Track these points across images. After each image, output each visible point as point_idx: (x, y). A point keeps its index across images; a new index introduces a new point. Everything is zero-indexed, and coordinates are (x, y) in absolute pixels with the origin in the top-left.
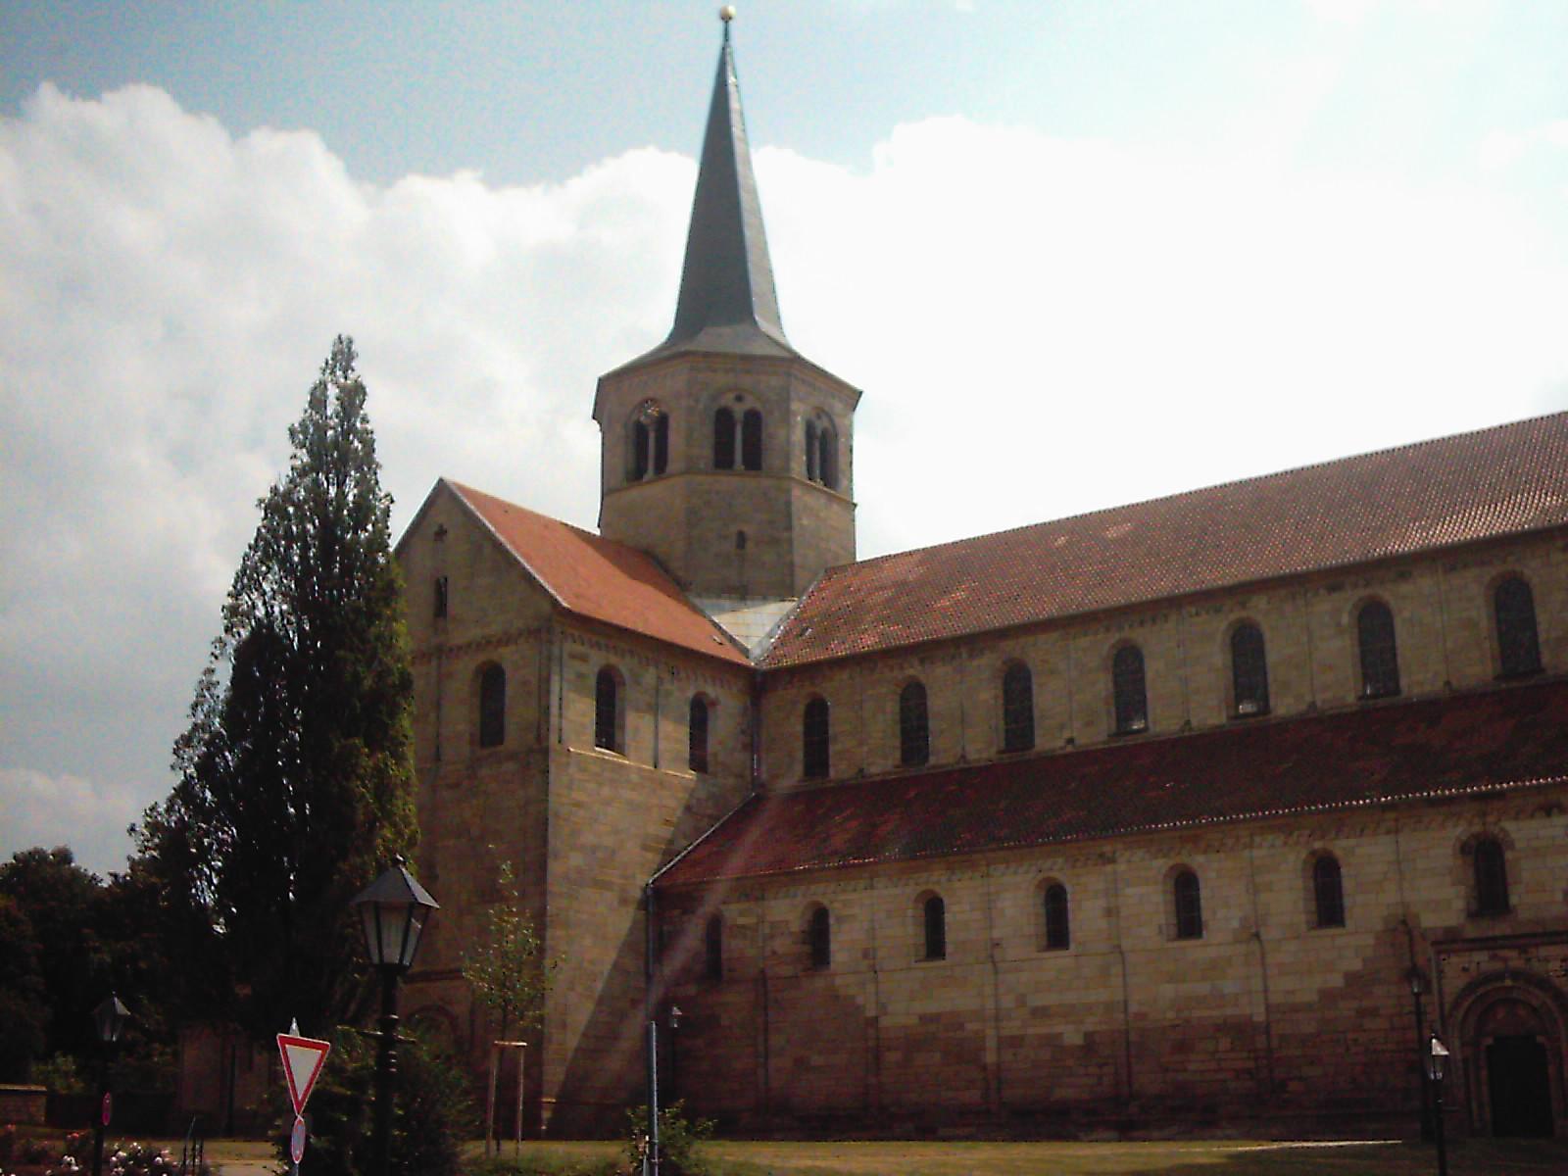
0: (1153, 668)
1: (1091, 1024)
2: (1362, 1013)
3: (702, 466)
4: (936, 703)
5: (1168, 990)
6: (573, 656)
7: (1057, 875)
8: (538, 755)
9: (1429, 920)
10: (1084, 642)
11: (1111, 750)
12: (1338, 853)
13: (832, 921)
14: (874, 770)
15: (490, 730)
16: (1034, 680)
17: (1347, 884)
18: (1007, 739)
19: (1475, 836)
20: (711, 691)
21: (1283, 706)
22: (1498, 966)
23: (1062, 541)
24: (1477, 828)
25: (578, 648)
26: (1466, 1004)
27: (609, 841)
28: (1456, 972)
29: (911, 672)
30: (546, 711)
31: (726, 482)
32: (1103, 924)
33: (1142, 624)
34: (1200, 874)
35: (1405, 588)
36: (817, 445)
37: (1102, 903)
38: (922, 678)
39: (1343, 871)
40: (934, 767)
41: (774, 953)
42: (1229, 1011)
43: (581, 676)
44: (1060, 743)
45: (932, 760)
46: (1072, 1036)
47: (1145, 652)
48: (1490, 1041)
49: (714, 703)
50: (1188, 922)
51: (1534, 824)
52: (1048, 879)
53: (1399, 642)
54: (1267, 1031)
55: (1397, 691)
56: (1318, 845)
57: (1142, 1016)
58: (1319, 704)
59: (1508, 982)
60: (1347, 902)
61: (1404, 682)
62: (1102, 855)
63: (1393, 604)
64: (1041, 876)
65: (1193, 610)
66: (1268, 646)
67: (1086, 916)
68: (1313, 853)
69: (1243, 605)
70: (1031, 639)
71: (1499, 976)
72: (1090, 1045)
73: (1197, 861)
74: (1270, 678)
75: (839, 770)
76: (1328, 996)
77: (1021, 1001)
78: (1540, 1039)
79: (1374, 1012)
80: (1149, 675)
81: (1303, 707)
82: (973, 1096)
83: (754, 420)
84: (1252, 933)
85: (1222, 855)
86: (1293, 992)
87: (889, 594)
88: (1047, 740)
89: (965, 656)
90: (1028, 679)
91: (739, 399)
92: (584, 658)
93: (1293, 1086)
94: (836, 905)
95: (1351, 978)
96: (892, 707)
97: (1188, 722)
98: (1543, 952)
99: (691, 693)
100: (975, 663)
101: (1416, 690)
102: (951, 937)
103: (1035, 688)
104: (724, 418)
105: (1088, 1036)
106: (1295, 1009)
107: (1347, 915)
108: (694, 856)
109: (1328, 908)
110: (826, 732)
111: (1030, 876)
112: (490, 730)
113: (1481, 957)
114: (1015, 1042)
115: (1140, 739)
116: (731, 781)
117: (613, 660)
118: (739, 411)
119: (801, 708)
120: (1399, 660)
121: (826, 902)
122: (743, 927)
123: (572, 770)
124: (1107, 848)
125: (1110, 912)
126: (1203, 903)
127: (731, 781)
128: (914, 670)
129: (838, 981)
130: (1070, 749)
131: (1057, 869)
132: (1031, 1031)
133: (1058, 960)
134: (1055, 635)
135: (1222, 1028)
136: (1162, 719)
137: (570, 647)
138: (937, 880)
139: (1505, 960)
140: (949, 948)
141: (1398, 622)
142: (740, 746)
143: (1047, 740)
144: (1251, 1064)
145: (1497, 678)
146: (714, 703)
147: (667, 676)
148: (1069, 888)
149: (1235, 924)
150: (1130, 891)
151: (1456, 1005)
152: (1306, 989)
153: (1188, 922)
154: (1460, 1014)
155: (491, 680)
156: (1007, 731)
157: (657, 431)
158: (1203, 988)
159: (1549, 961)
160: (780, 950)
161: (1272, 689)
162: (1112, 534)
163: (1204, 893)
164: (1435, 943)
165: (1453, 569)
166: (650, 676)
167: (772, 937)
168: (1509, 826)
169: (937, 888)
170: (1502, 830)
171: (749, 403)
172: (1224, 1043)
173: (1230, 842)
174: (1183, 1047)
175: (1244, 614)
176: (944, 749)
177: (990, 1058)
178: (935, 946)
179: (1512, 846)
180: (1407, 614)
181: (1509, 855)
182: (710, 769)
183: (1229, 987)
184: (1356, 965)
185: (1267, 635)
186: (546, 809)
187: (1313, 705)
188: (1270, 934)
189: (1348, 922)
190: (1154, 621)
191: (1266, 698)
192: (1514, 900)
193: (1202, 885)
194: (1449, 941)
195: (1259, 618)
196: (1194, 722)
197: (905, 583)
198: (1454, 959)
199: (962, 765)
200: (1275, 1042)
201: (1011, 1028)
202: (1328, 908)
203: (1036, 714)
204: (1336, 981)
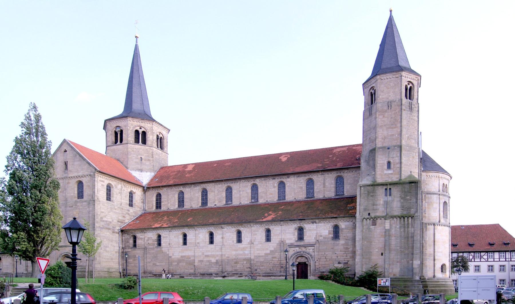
0: (234, 192)
1: (217, 258)
2: (273, 258)
3: (131, 142)
4: (186, 196)
5: (234, 253)
6: (100, 181)
7: (212, 230)
8: (93, 201)
9: (288, 242)
10: (220, 186)
11: (224, 207)
12: (271, 229)
13: (162, 237)
14: (172, 208)
15: (80, 195)
16: (208, 192)
17: (272, 235)
18: (202, 204)
19: (298, 227)
20: (134, 190)
21: (261, 201)
22: (300, 250)
23: (215, 165)
24: (299, 225)
25: (102, 179)
26: (293, 257)
27: (110, 220)
28: (292, 251)
29: (181, 189)
30: (94, 192)
31: (137, 146)
32: (221, 240)
33: (232, 183)
34: (242, 232)
35: (289, 180)
36: (159, 140)
37: (221, 236)
38: (183, 191)
39: (271, 232)
40: (185, 209)
41: (148, 243)
42: (246, 257)
43: (102, 185)
44: (213, 205)
45: (185, 207)
46: (213, 260)
47: (233, 188)
48: (298, 263)
49: (134, 193)
50: (239, 240)
51: (310, 225)
52: (210, 231)
53: (286, 190)
54: (254, 260)
55: (285, 199)
56: (267, 227)
57: (229, 257)
58: (268, 201)
59: (302, 253)
60: (272, 238)
61: (286, 198)
62: (222, 227)
63: (285, 182)
64: (208, 231)
65: (244, 181)
66: (259, 189)
67: (217, 238)
68: (266, 228)
69: (254, 181)
70: (208, 184)
71: (301, 252)
72: (217, 262)
73: (241, 229)
74: (259, 195)
75: (164, 208)
76: (267, 254)
77: (203, 254)
78: (307, 263)
79: (275, 257)
80: (233, 193)
81: (265, 201)
82: (192, 271)
83: (144, 133)
84: (251, 243)
85: (247, 228)
86: (259, 253)
87: (175, 173)
88: (210, 205)
89: (193, 187)
90: (207, 192)
91: (141, 128)
92: (103, 182)
93: (258, 270)
94: (163, 234)
95: (271, 251)
96: (176, 196)
97: (241, 203)
98: (309, 248)
99: (129, 190)
100: (195, 188)
101: (289, 199)
102: (188, 241)
103: (208, 194)
104: (137, 132)
105: (216, 260)
106: (259, 256)
107: (271, 240)
108: (129, 224)
109: (268, 239)
110: (161, 200)
111: (206, 231)
112: (80, 195)
113: (298, 248)
114: (201, 261)
115: (230, 205)
116: (139, 209)
117: (110, 182)
118: (141, 131)
119: (155, 195)
120: (286, 194)
121: (161, 234)
122: (142, 238)
123: (101, 205)
124: (223, 226)
125: (223, 238)
126: (242, 237)
127: (139, 209)
128: (181, 188)
129: (163, 249)
130: (215, 207)
131: (212, 229)
132: (205, 259)
133: (212, 245)
134: (213, 184)
135: (245, 259)
136: (235, 202)
137: (99, 178)
138: (186, 230)
139: (302, 249)
140: (188, 244)
141: (286, 186)
142: (141, 202)
143: (210, 205)
144: (250, 266)
145: (305, 198)
146: (134, 193)
147: (124, 187)
148: (214, 233)
149: (249, 241)
150: (227, 234)
151: (291, 257)
152: (262, 253)
153: (239, 240)
154: (292, 258)
155: (80, 184)
156: (202, 202)
157: (120, 134)
158: (241, 252)
159: (310, 250)
160: (150, 243)
161: (259, 197)
162: (227, 164)
163: (243, 235)
164: (288, 246)
165: (299, 177)
166: (119, 186)
167: (148, 240)
168: (305, 225)
169: (185, 232)
170: (304, 226)
171: (143, 130)
172: (245, 262)
173: (249, 226)
174: (236, 263)
175: (254, 182)
176: (187, 205)
177: (196, 264)
178: (185, 243)
179: (305, 229)
180: (288, 185)
181: (304, 230)
182: (134, 206)
183: (246, 252)
184: (273, 249)
185: (259, 187)
186: (94, 213)
187: (267, 201)
188: (256, 243)
189: (272, 241)
190: (235, 182)
191: (258, 199)
192: (305, 238)
193: (242, 233)
194: (291, 246)
195: (257, 183)
196: (242, 203)
197: (180, 171)
198: (292, 248)
199: (191, 209)
200: (255, 262)
201: (201, 259)
202: (268, 239)
203: (208, 199)
204: (268, 252)
